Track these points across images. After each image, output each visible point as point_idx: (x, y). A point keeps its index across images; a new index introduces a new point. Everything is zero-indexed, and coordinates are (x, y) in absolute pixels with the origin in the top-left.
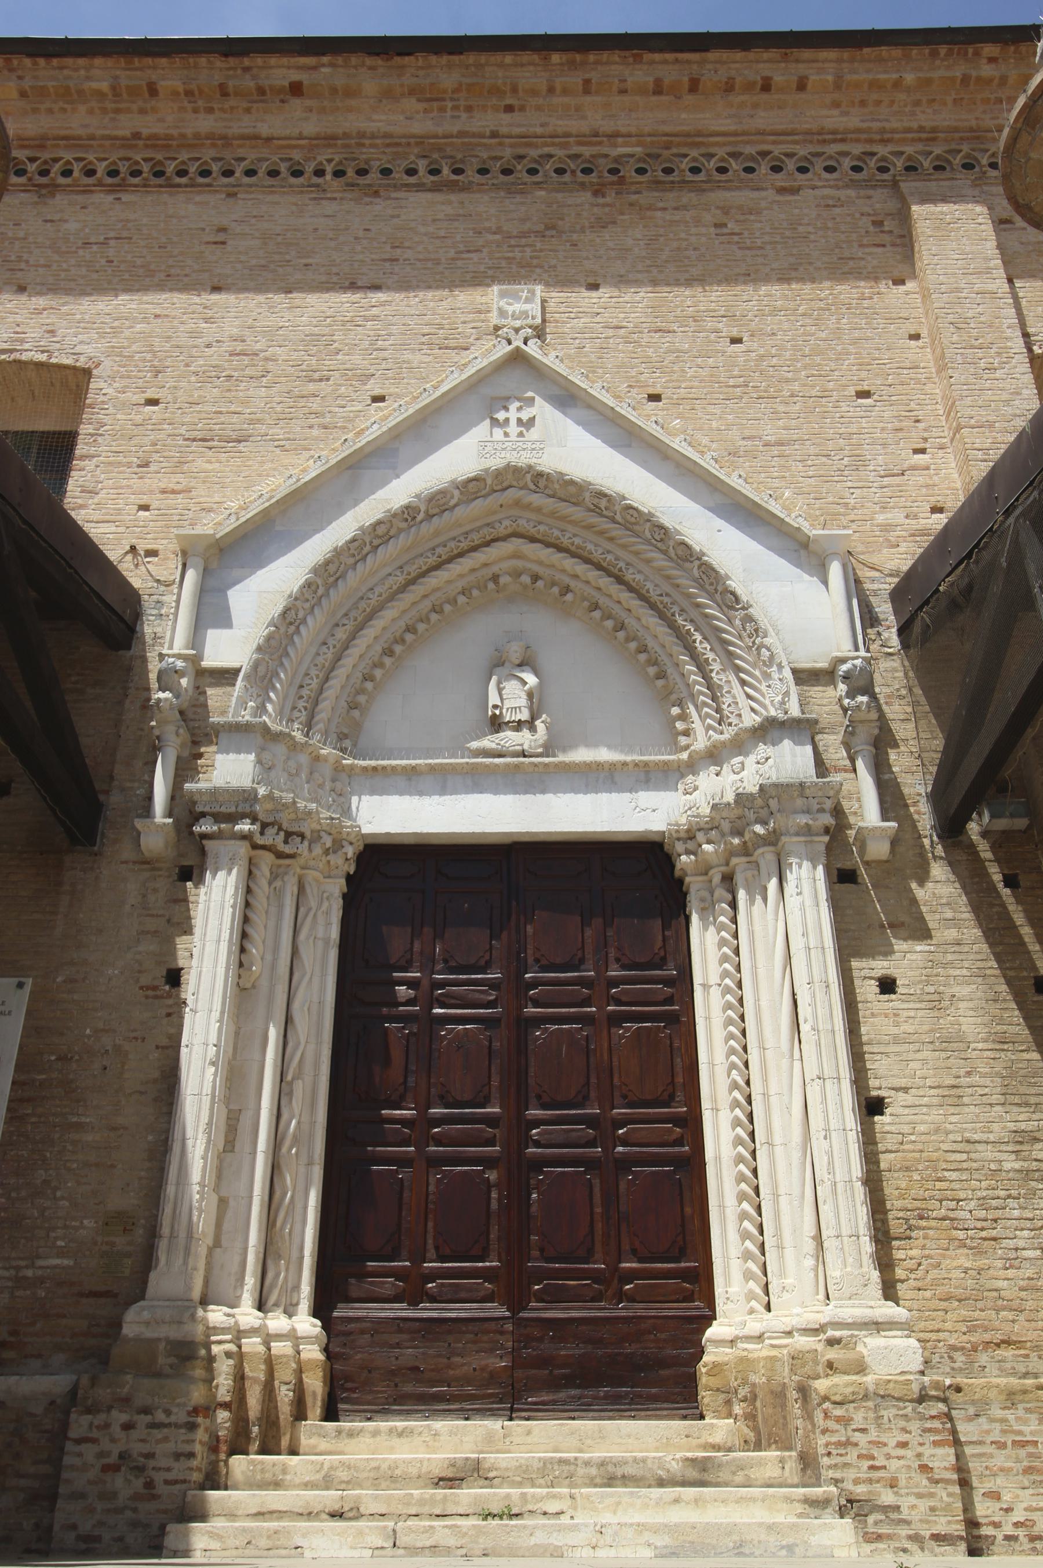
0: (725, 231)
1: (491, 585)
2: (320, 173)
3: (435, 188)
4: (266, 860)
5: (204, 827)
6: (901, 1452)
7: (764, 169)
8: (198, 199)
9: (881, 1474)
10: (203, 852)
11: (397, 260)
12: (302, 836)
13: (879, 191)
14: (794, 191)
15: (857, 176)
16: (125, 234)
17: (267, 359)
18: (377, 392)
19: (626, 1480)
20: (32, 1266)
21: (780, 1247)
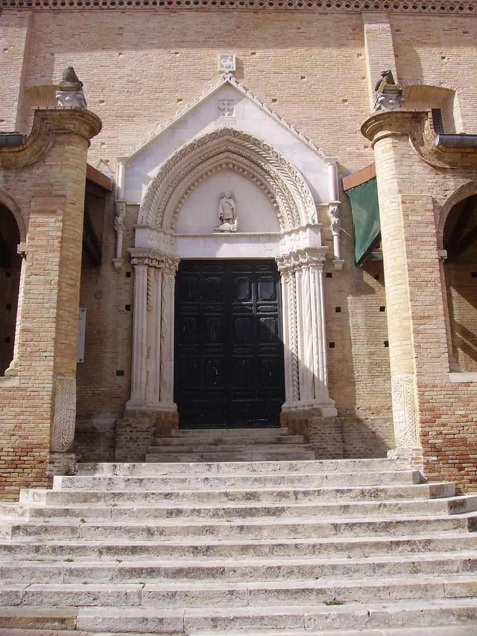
0: (300, 31)
1: (219, 168)
3: (197, 10)
4: (153, 270)
5: (135, 261)
6: (329, 435)
9: (324, 440)
10: (134, 268)
11: (184, 42)
12: (163, 262)
16: (86, 30)
17: (140, 84)
18: (179, 98)
19: (259, 443)
20: (97, 390)
21: (303, 384)
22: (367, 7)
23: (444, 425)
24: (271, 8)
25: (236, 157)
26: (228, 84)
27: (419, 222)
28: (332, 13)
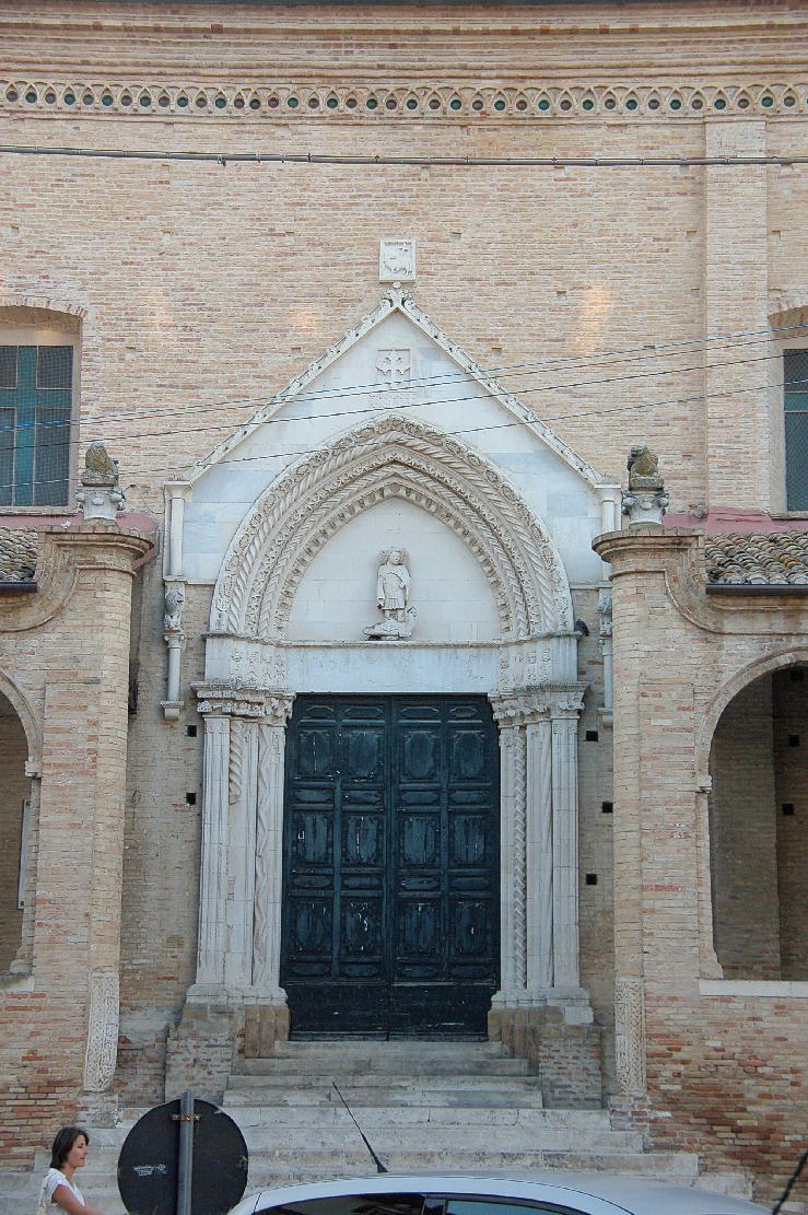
3: (333, 122)
4: (239, 723)
5: (204, 707)
6: (575, 1061)
8: (143, 129)
9: (565, 1071)
11: (304, 204)
20: (131, 963)
22: (720, 104)
23: (684, 1062)
24: (501, 114)
25: (411, 474)
26: (397, 310)
27: (665, 729)
28: (637, 126)
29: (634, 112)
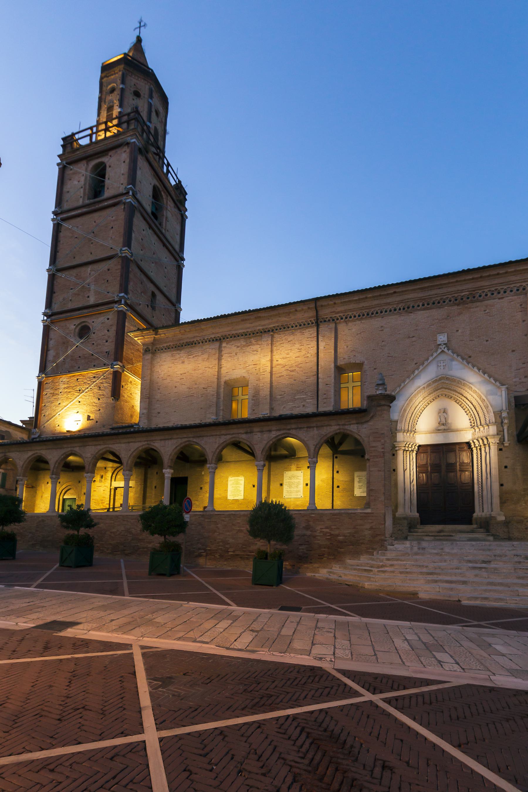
2: (400, 309)
3: (424, 309)
7: (495, 294)
8: (376, 319)
13: (523, 296)
14: (502, 298)
15: (518, 292)
28: (507, 297)
29: (506, 294)
